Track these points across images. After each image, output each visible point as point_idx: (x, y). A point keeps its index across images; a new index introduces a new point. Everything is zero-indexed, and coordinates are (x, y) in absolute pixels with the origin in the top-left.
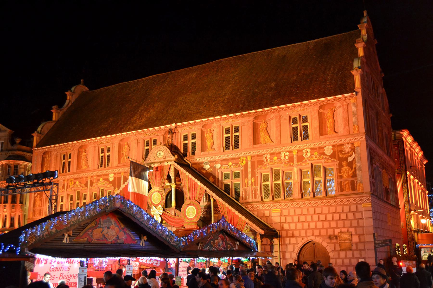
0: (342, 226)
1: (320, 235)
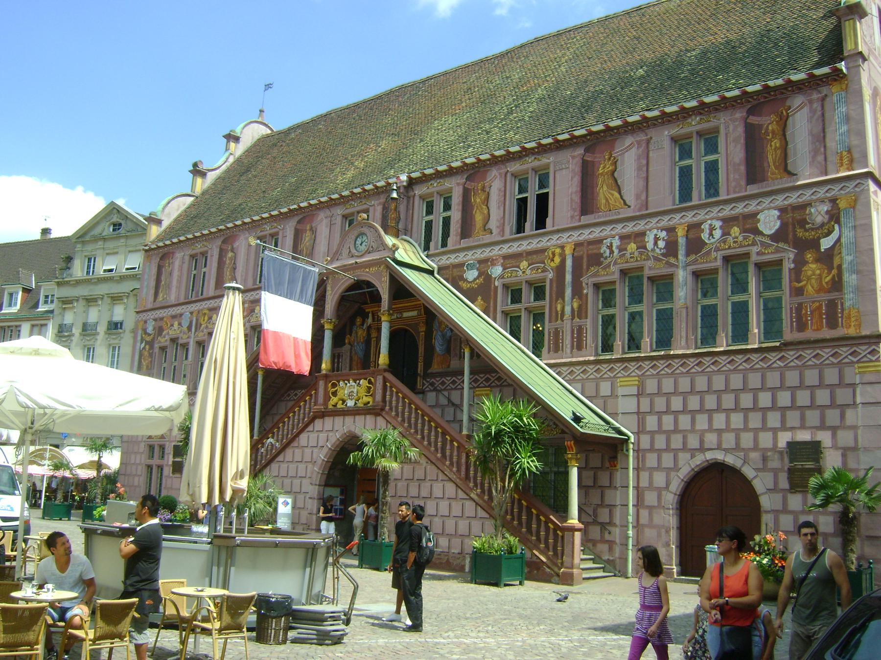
0: (797, 424)
1: (738, 447)
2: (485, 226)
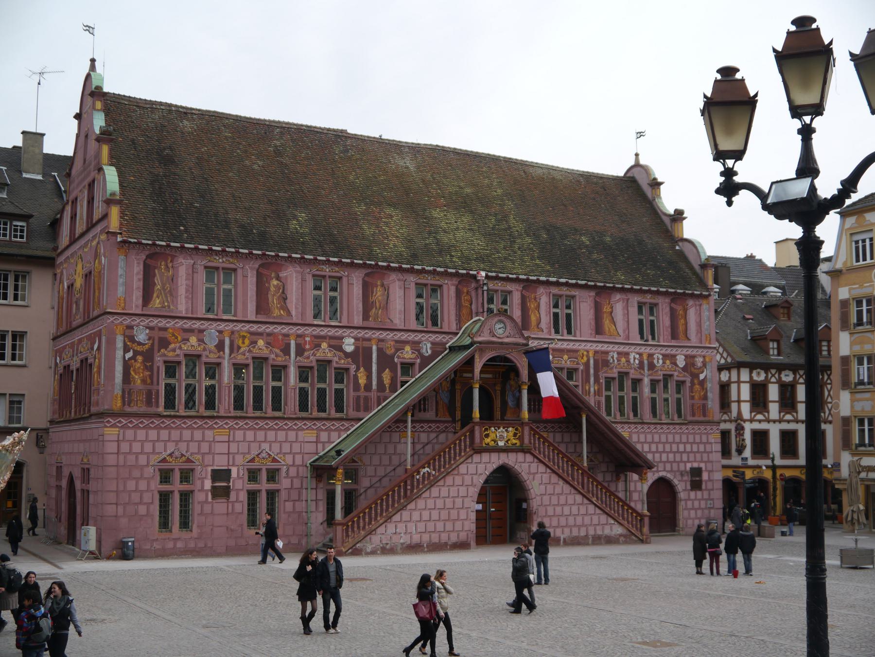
2: (538, 326)
